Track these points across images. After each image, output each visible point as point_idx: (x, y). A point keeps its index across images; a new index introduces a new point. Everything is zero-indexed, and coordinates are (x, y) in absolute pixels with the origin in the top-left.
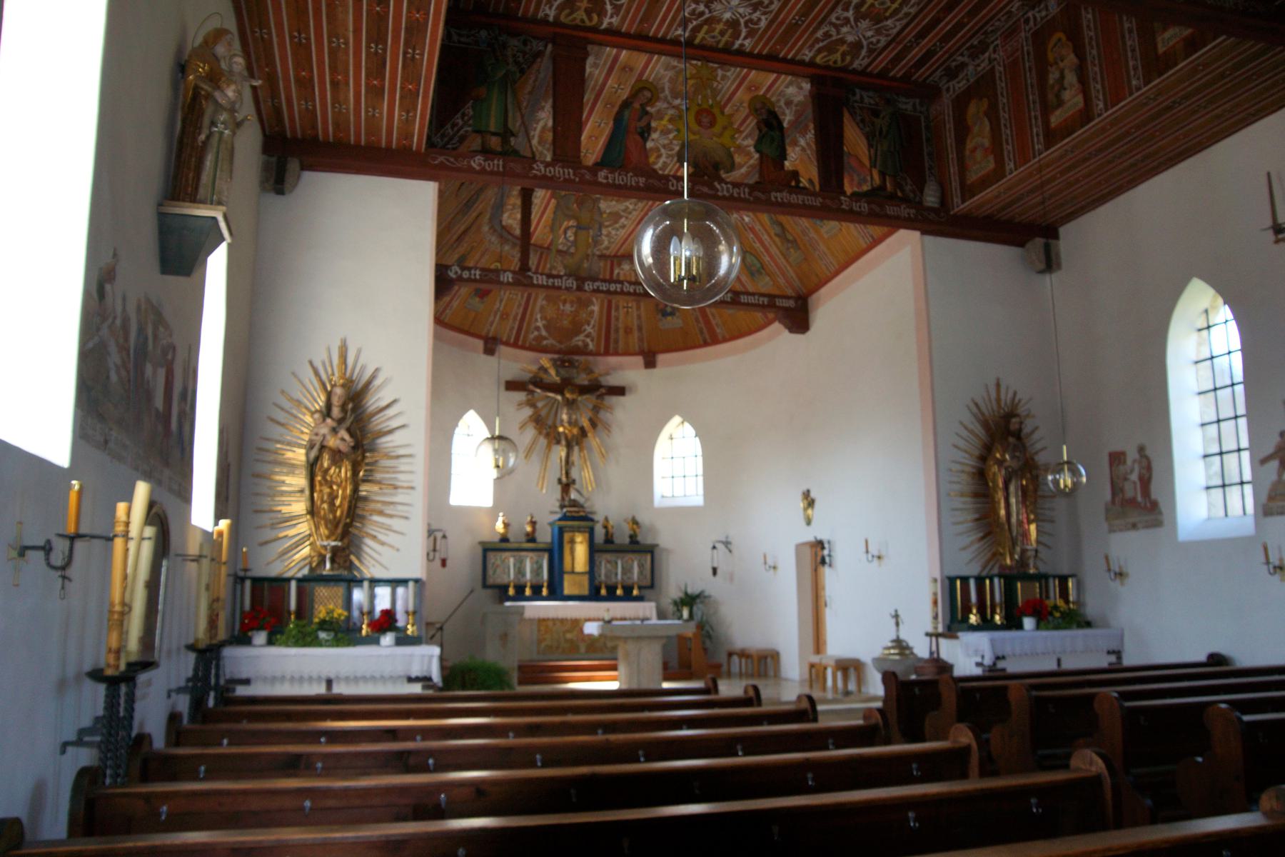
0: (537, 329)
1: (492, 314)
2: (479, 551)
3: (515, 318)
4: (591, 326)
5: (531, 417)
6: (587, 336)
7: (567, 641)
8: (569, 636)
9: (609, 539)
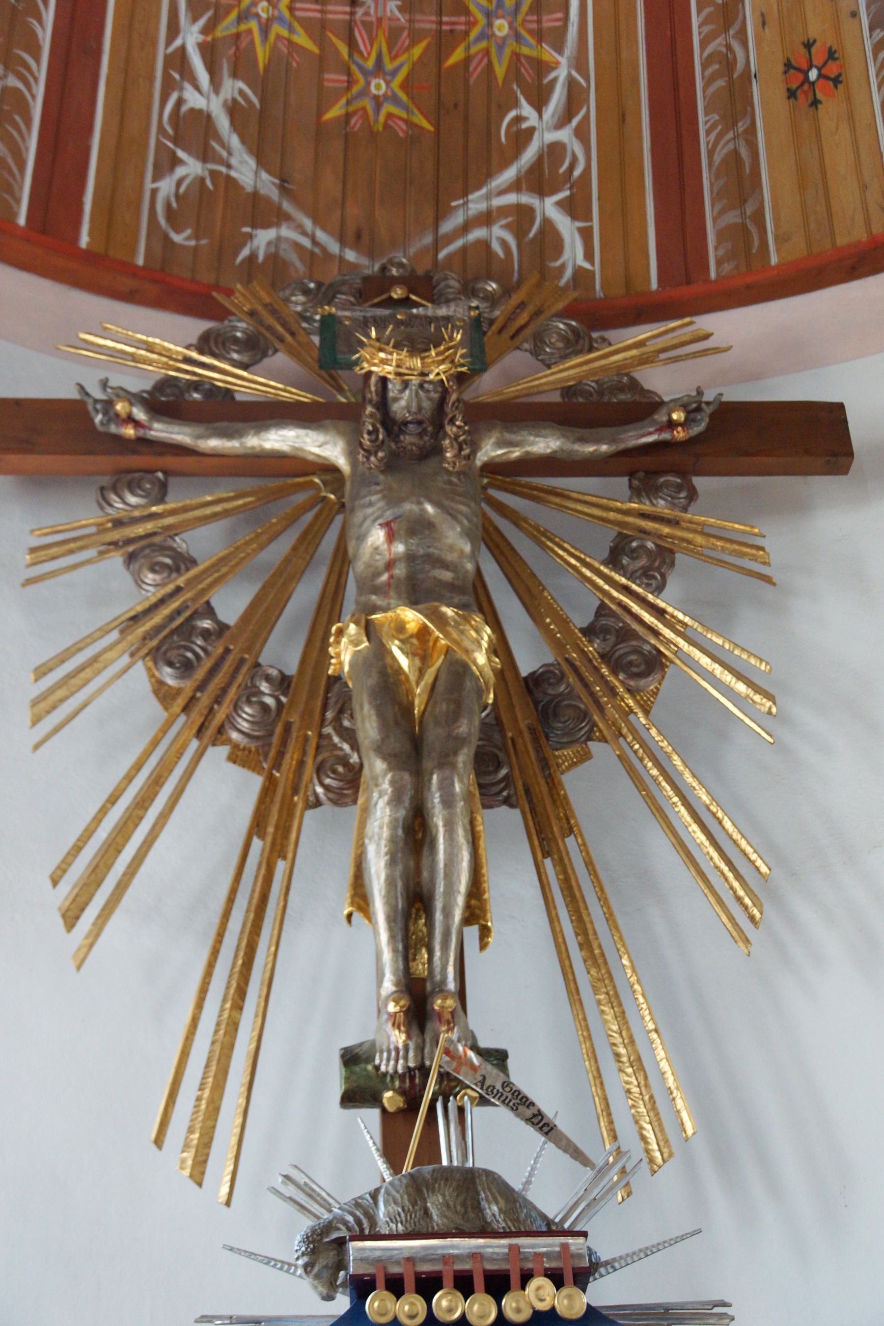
4: (558, 97)
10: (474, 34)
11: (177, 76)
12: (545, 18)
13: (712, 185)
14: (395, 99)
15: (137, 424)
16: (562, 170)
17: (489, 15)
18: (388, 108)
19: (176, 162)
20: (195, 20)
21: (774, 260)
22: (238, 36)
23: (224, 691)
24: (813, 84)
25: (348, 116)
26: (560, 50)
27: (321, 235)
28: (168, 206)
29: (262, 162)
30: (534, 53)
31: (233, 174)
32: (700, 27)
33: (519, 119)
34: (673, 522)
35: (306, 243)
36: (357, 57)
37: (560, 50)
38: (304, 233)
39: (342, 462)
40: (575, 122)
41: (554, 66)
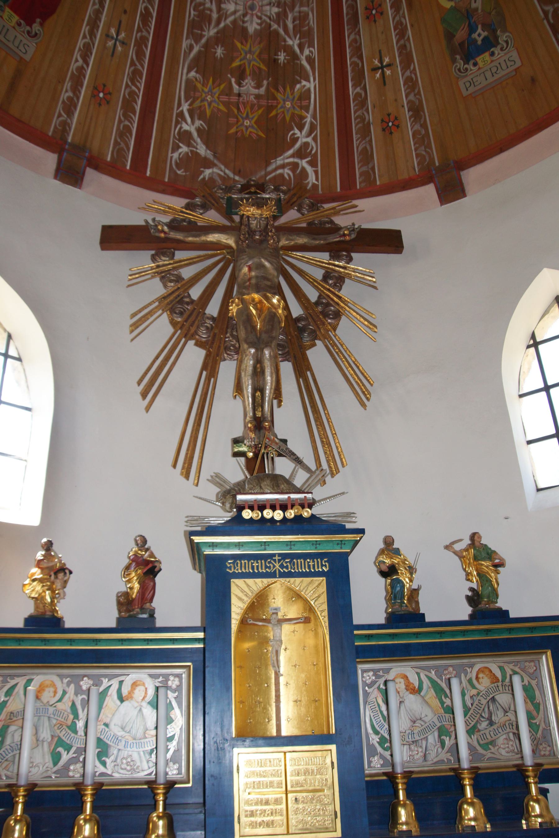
0: (186, 137)
1: (68, 84)
3: (128, 106)
6: (301, 154)
10: (279, 106)
11: (180, 120)
12: (303, 102)
13: (358, 158)
14: (253, 127)
15: (165, 233)
16: (308, 151)
17: (284, 101)
18: (250, 129)
19: (179, 147)
20: (186, 101)
21: (378, 183)
22: (200, 107)
23: (194, 322)
24: (390, 127)
25: (237, 132)
26: (308, 112)
27: (227, 171)
28: (176, 162)
29: (208, 147)
30: (299, 113)
31: (198, 151)
32: (354, 107)
33: (294, 134)
35: (222, 174)
36: (240, 113)
37: (308, 112)
38: (221, 171)
39: (233, 245)
40: (313, 135)
41: (306, 117)
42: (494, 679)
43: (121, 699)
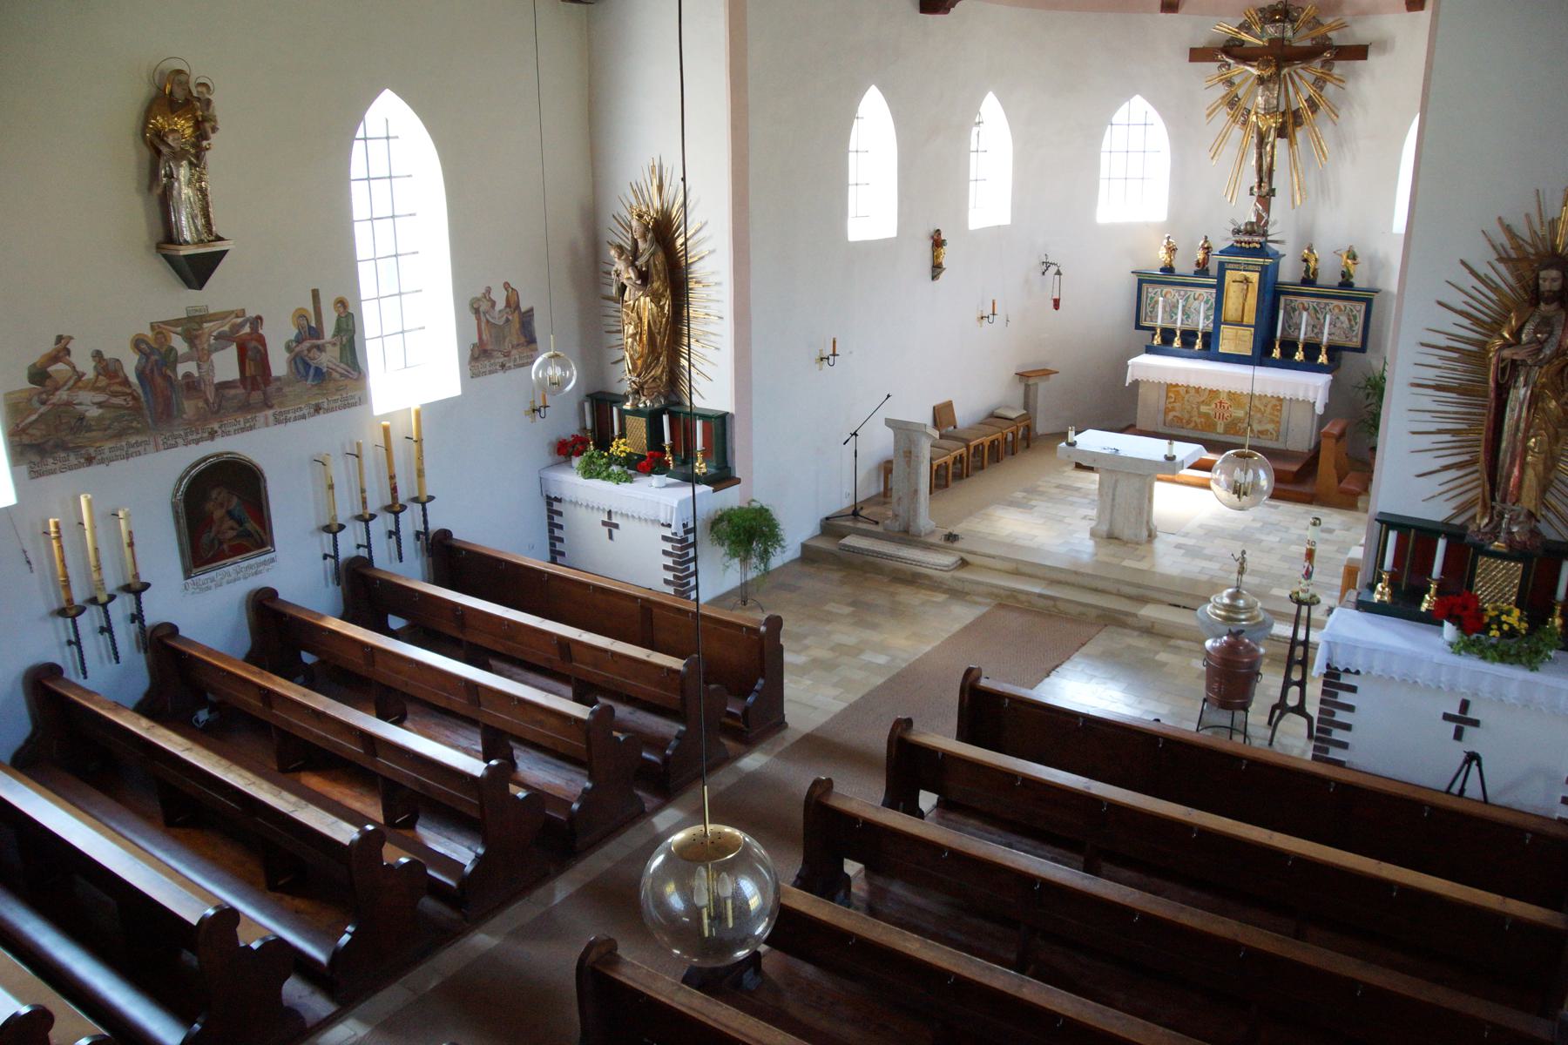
2: (1135, 279)
5: (1224, 97)
7: (1200, 414)
8: (1204, 409)
9: (1309, 280)
34: (1328, 75)
42: (1340, 310)
43: (1195, 299)
